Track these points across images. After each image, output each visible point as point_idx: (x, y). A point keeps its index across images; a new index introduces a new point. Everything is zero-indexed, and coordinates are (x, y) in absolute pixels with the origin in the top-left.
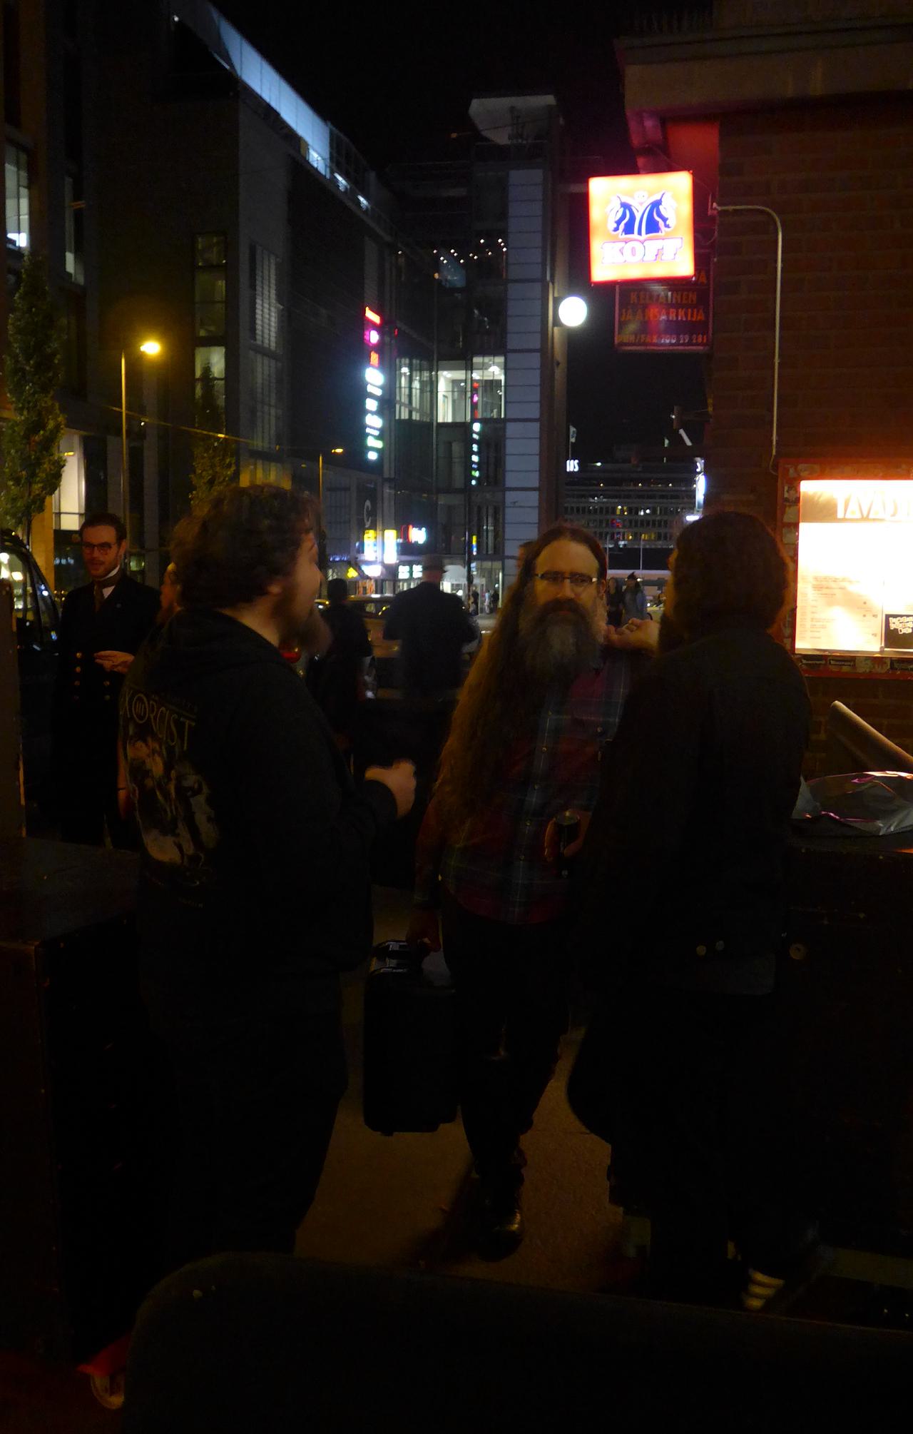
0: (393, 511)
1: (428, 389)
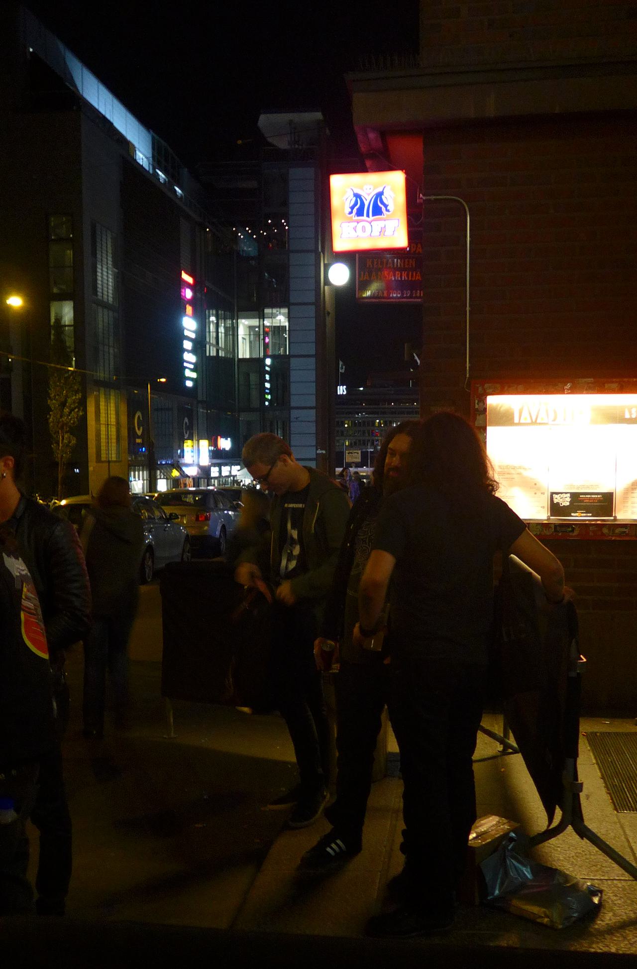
1: (231, 333)
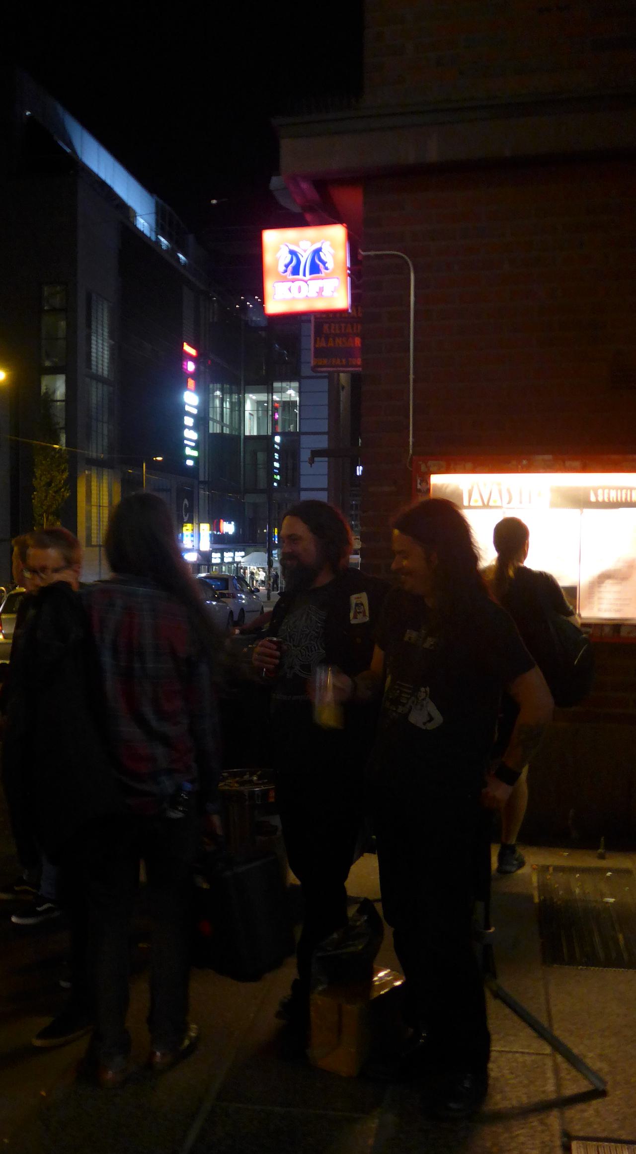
0: (207, 508)
1: (237, 409)
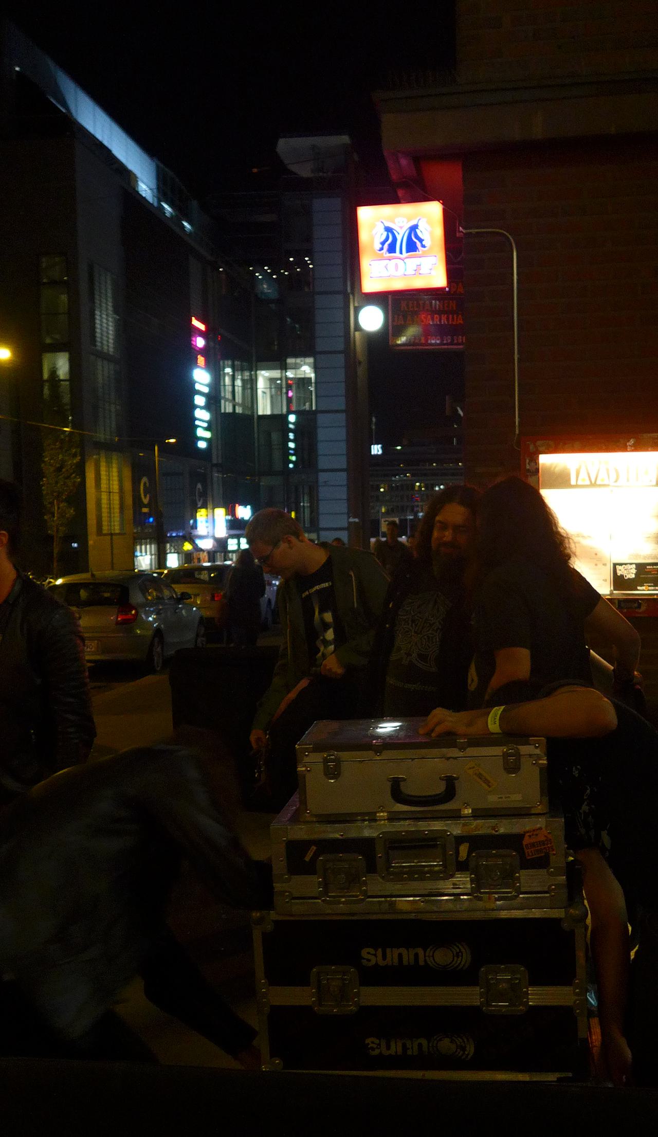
0: (221, 492)
